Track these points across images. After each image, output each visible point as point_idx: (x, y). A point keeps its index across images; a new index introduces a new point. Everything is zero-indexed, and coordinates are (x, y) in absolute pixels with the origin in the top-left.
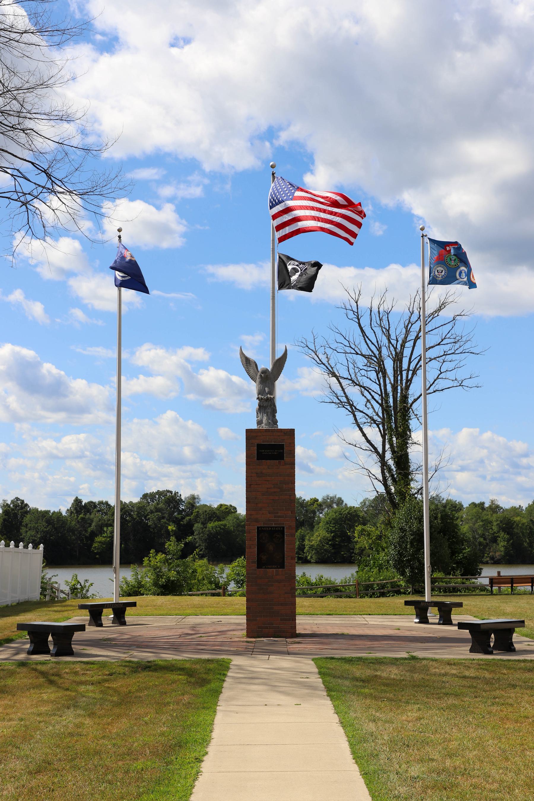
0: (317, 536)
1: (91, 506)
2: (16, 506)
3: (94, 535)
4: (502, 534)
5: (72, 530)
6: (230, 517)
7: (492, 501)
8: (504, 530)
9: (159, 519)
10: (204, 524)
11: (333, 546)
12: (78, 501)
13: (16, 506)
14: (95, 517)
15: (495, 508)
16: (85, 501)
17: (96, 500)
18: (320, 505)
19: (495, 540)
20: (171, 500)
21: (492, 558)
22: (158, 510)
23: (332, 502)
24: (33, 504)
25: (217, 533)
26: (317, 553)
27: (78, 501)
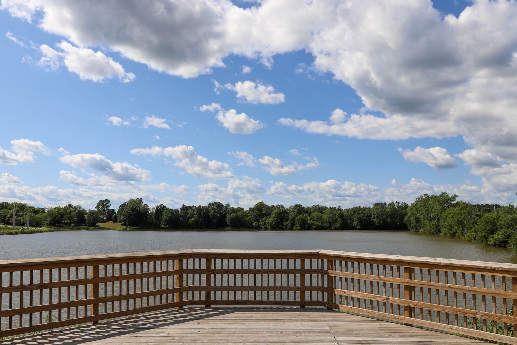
0: (271, 219)
1: (190, 207)
2: (161, 207)
3: (189, 218)
4: (339, 219)
5: (180, 216)
6: (240, 212)
7: (339, 207)
8: (340, 217)
9: (214, 213)
10: (230, 214)
11: (277, 223)
12: (184, 206)
13: (161, 207)
14: (189, 211)
15: (340, 209)
16: (187, 206)
17: (191, 205)
18: (275, 208)
19: (336, 221)
20: (219, 205)
21: (335, 228)
22: (213, 209)
23: (280, 207)
24: (168, 206)
25: (234, 218)
26: (271, 225)
27: (184, 206)
